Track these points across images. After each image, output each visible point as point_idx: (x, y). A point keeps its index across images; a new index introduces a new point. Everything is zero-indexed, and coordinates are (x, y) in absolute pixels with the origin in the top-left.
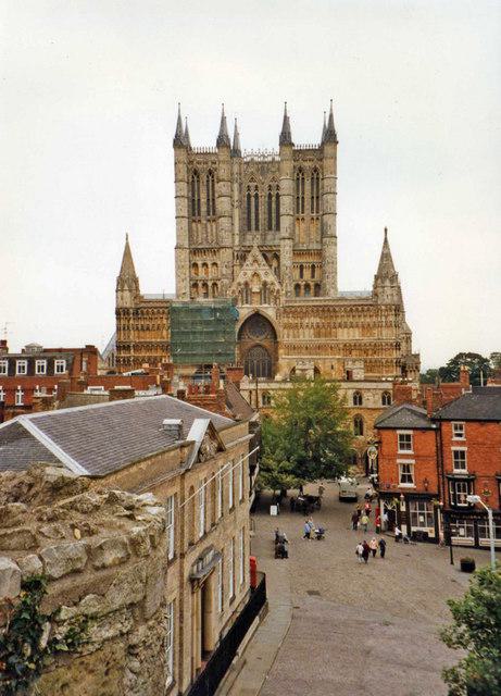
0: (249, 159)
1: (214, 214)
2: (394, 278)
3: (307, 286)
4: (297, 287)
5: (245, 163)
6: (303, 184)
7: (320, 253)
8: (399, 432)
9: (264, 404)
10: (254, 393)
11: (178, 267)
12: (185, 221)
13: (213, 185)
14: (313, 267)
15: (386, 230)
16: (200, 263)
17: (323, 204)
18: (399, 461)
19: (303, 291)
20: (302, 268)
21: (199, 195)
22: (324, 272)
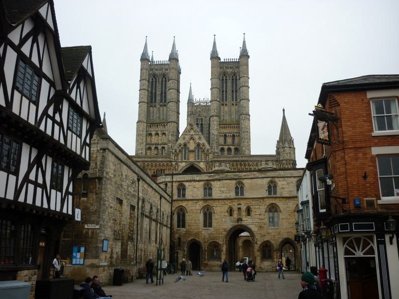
0: (197, 104)
1: (165, 101)
2: (291, 141)
3: (229, 149)
4: (222, 150)
5: (195, 106)
6: (226, 83)
7: (237, 124)
8: (370, 95)
9: (179, 196)
10: (169, 185)
11: (138, 135)
12: (145, 105)
14: (234, 136)
15: (284, 110)
16: (153, 133)
17: (240, 95)
18: (376, 151)
19: (226, 152)
20: (225, 136)
21: (156, 90)
22: (240, 140)
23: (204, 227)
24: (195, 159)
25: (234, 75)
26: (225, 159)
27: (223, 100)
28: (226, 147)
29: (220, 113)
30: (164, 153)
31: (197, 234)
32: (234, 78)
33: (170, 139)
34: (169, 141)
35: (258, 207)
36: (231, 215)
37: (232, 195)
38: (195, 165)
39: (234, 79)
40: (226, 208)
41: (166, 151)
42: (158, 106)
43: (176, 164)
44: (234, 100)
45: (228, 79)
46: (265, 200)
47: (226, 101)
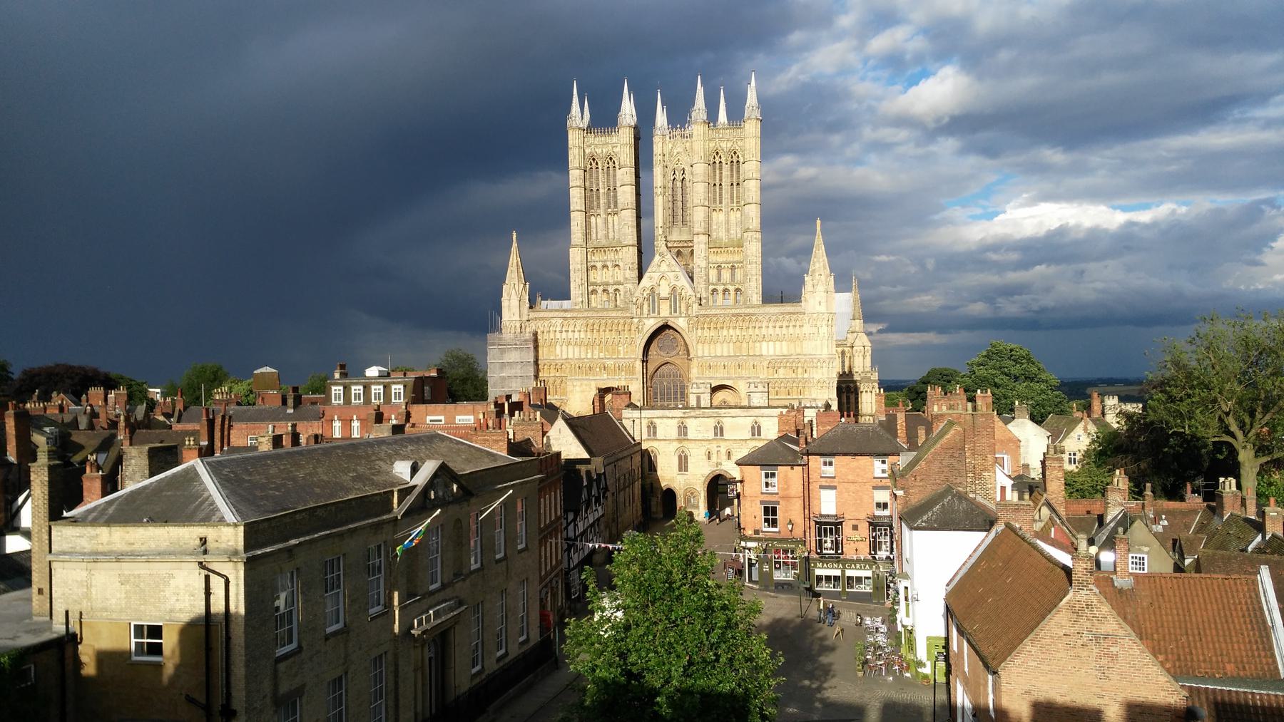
1: (616, 206)
3: (725, 291)
6: (721, 169)
10: (637, 422)
13: (615, 171)
16: (599, 265)
23: (679, 471)
24: (671, 313)
25: (735, 153)
26: (718, 312)
27: (715, 202)
28: (720, 288)
29: (709, 225)
30: (618, 299)
31: (672, 479)
32: (735, 159)
33: (627, 276)
34: (626, 279)
35: (740, 450)
36: (709, 458)
37: (711, 435)
38: (669, 323)
39: (735, 161)
40: (703, 451)
41: (622, 296)
42: (603, 216)
43: (639, 322)
44: (735, 201)
45: (724, 162)
46: (748, 442)
47: (721, 203)
